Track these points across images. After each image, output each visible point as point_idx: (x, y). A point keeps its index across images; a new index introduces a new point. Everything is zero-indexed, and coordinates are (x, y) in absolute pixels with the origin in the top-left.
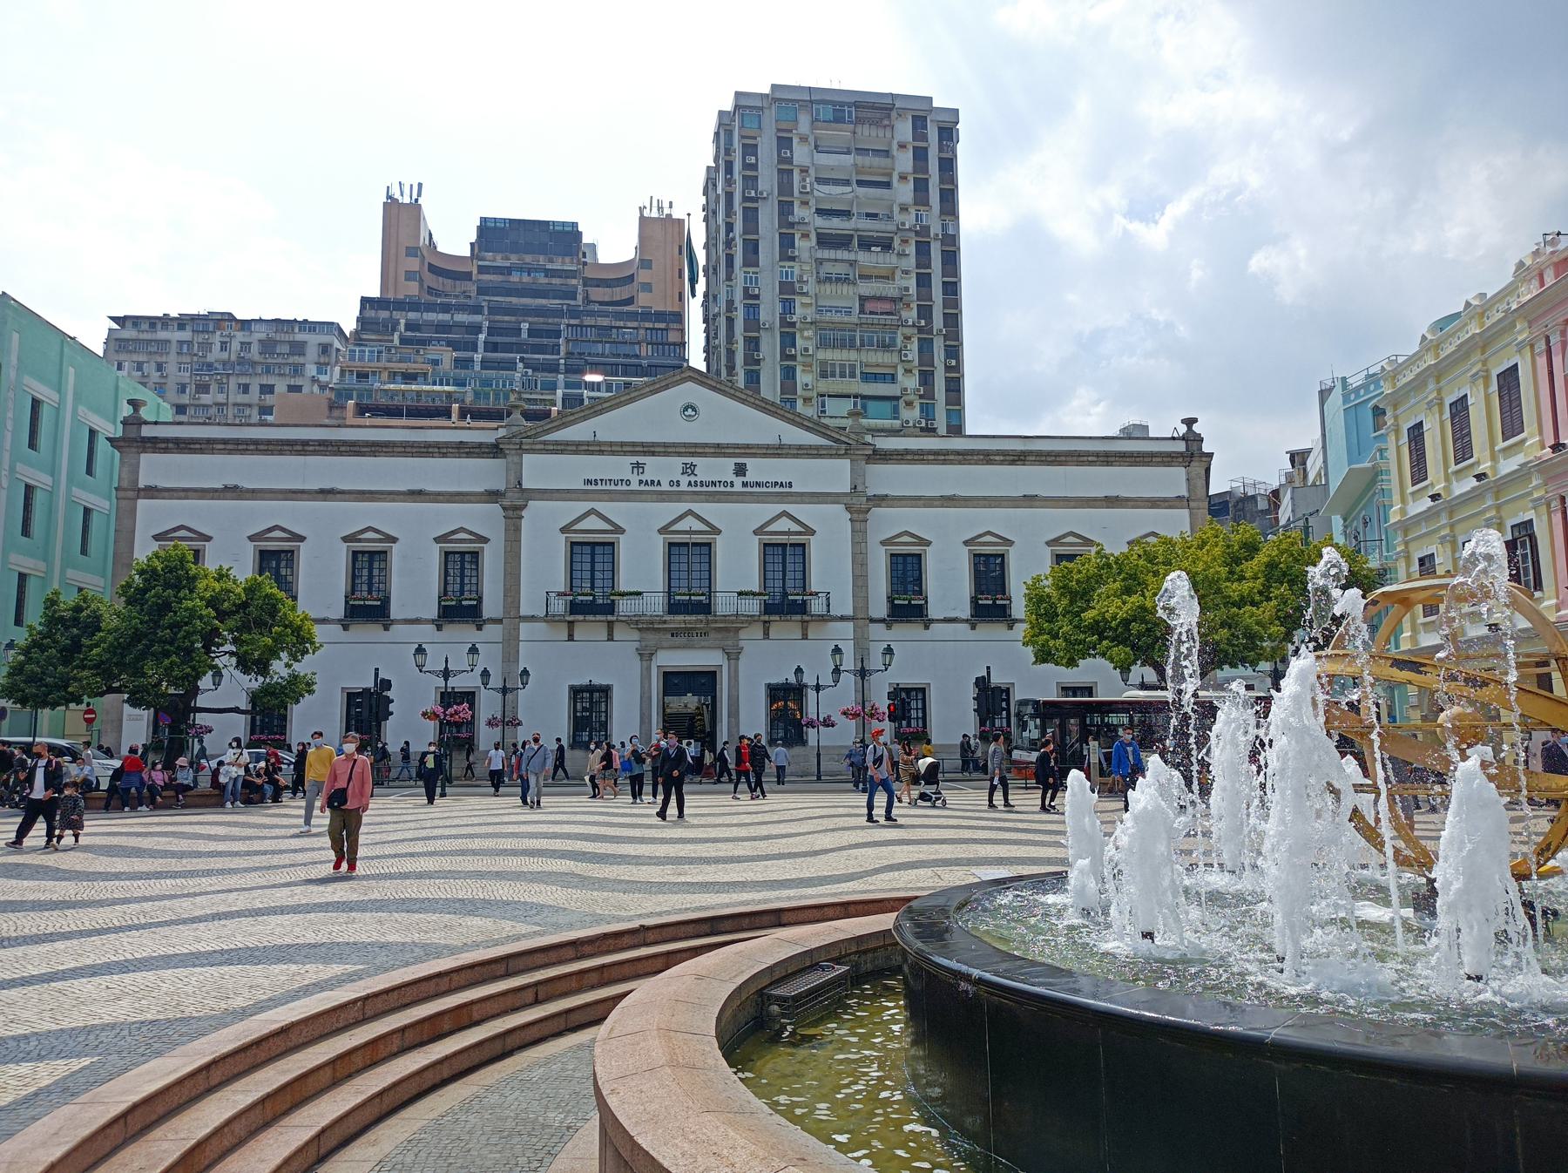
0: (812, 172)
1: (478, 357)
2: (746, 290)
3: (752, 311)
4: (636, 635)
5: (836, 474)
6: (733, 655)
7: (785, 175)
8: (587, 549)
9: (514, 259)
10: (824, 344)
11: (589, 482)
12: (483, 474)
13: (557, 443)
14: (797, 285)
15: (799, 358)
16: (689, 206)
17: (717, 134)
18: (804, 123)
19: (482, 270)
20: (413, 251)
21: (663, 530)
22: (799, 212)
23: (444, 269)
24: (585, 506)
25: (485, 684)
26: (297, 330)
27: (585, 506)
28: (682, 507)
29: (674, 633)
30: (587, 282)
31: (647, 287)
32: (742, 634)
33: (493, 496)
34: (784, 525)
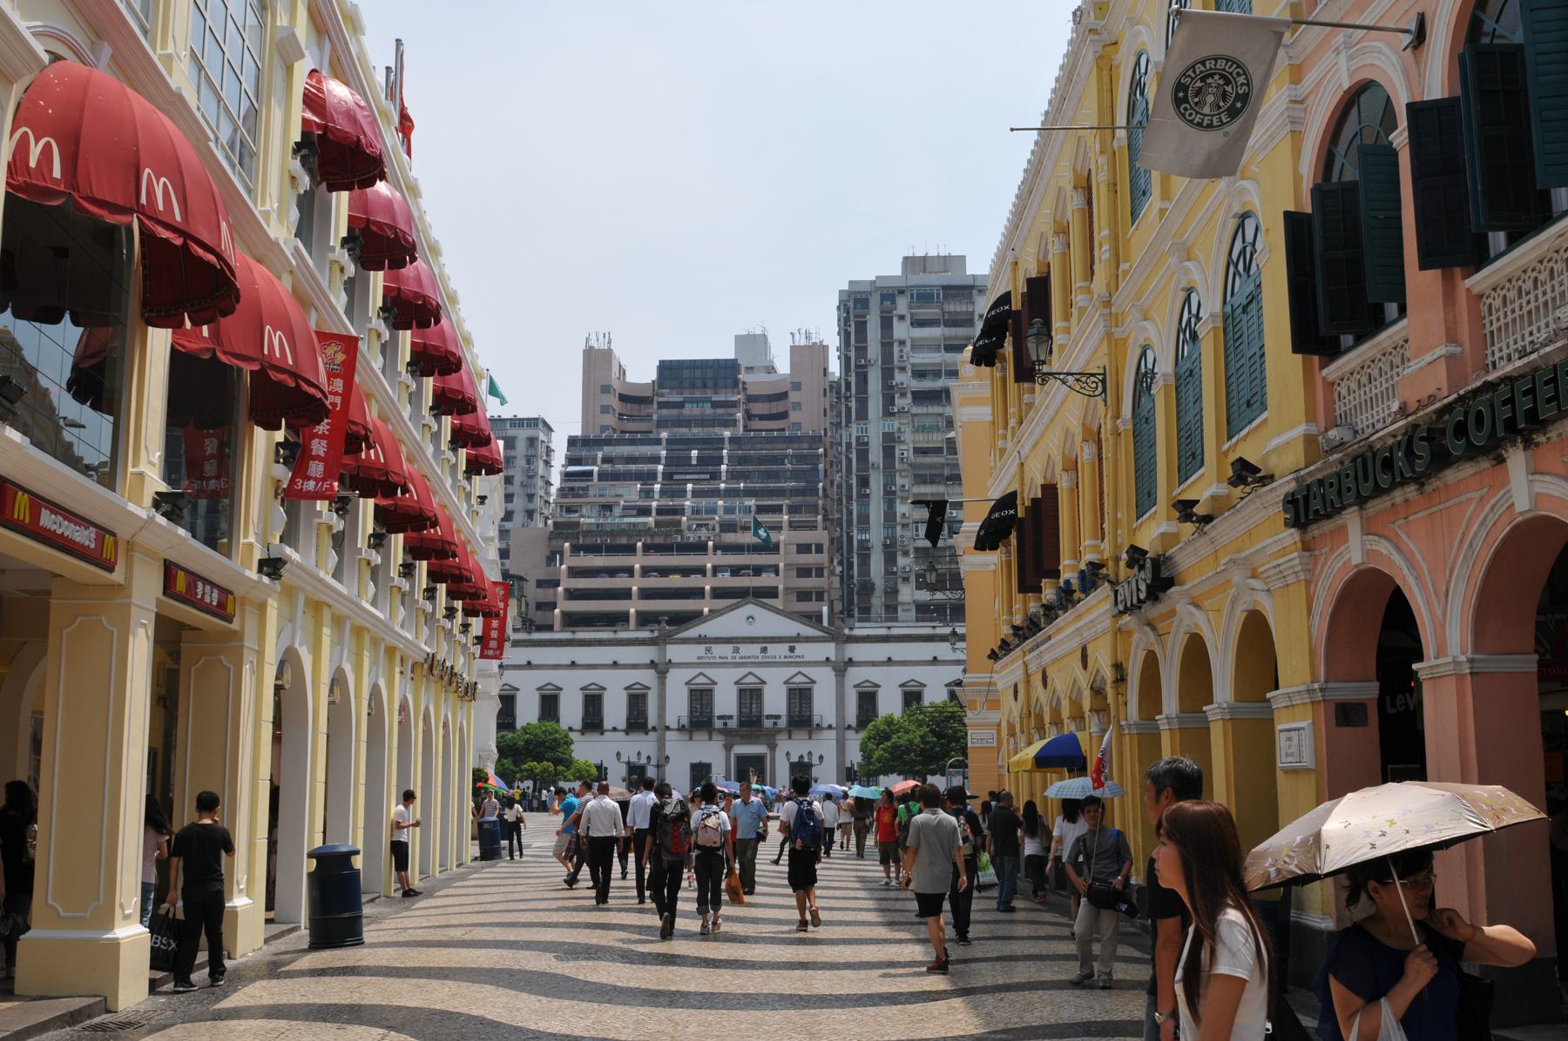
0: (908, 343)
1: (657, 487)
2: (858, 438)
3: (863, 454)
4: (723, 738)
5: (828, 650)
6: (773, 747)
7: (887, 345)
8: (698, 693)
9: (687, 395)
10: (921, 480)
11: (699, 658)
12: (645, 654)
13: (682, 639)
14: (896, 435)
15: (899, 493)
16: (830, 335)
17: (839, 308)
18: (902, 306)
19: (662, 405)
20: (606, 389)
21: (737, 683)
22: (899, 378)
23: (633, 399)
24: (698, 671)
25: (649, 763)
26: (508, 426)
27: (698, 671)
28: (746, 670)
29: (742, 737)
30: (751, 399)
31: (797, 406)
32: (778, 737)
33: (653, 664)
34: (800, 679)
